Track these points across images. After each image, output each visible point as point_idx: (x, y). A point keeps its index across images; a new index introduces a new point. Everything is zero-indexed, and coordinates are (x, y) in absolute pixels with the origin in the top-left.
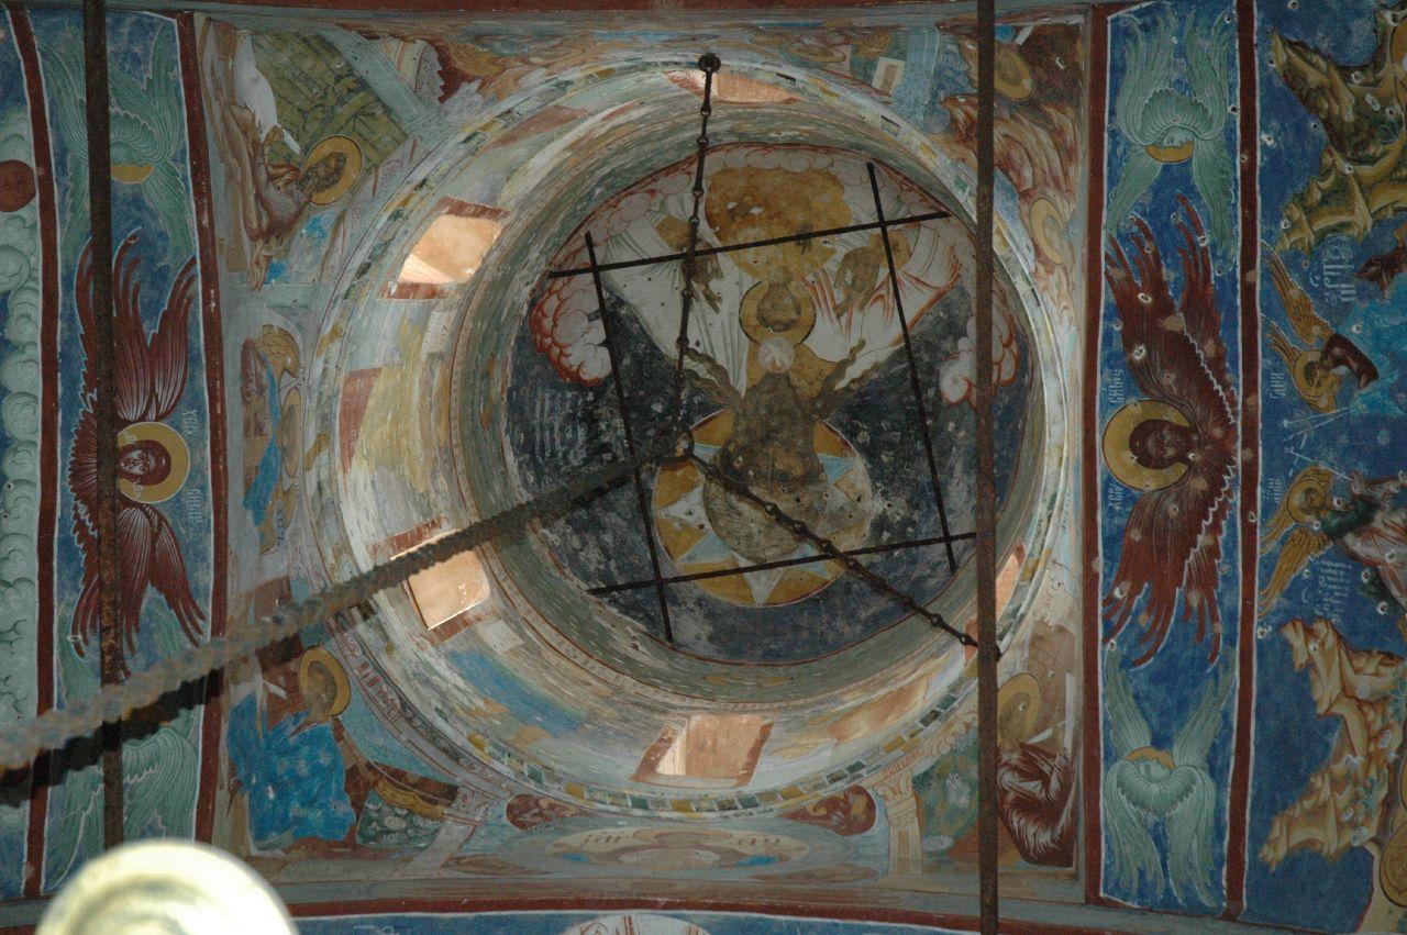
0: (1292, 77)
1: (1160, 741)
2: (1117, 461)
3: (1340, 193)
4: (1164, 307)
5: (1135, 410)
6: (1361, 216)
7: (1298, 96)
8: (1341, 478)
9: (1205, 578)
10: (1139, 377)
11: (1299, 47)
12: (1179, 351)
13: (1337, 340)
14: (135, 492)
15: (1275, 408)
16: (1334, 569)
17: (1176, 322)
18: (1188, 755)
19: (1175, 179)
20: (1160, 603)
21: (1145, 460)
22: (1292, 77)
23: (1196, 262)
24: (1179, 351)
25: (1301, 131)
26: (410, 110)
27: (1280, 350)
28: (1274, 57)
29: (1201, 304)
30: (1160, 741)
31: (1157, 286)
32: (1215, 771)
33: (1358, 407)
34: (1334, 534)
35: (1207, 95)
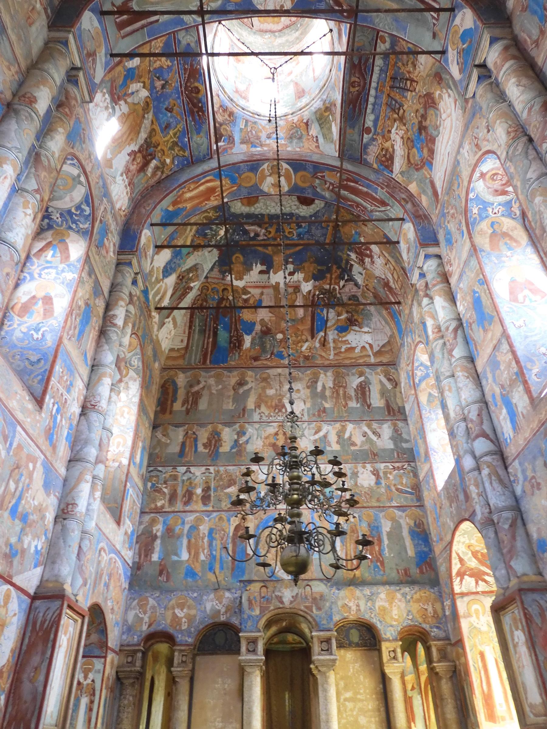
0: (184, 152)
1: (188, 44)
2: (201, 87)
3: (175, 134)
4: (198, 112)
5: (200, 96)
6: (171, 133)
7: (183, 149)
8: (168, 90)
9: (185, 70)
10: (200, 101)
11: (184, 156)
12: (195, 105)
13: (171, 112)
14: (357, 80)
15: (179, 98)
16: (166, 76)
17: (195, 110)
18: (184, 42)
19: (198, 133)
20: (192, 65)
21: (197, 88)
22: (184, 152)
23: (194, 120)
24: (195, 105)
25: (182, 142)
26: (313, 118)
27: (180, 107)
28: (187, 154)
29: (192, 113)
30: (188, 44)
31: (199, 115)
32: (179, 40)
33: (167, 103)
34: (167, 82)
35: (195, 145)
